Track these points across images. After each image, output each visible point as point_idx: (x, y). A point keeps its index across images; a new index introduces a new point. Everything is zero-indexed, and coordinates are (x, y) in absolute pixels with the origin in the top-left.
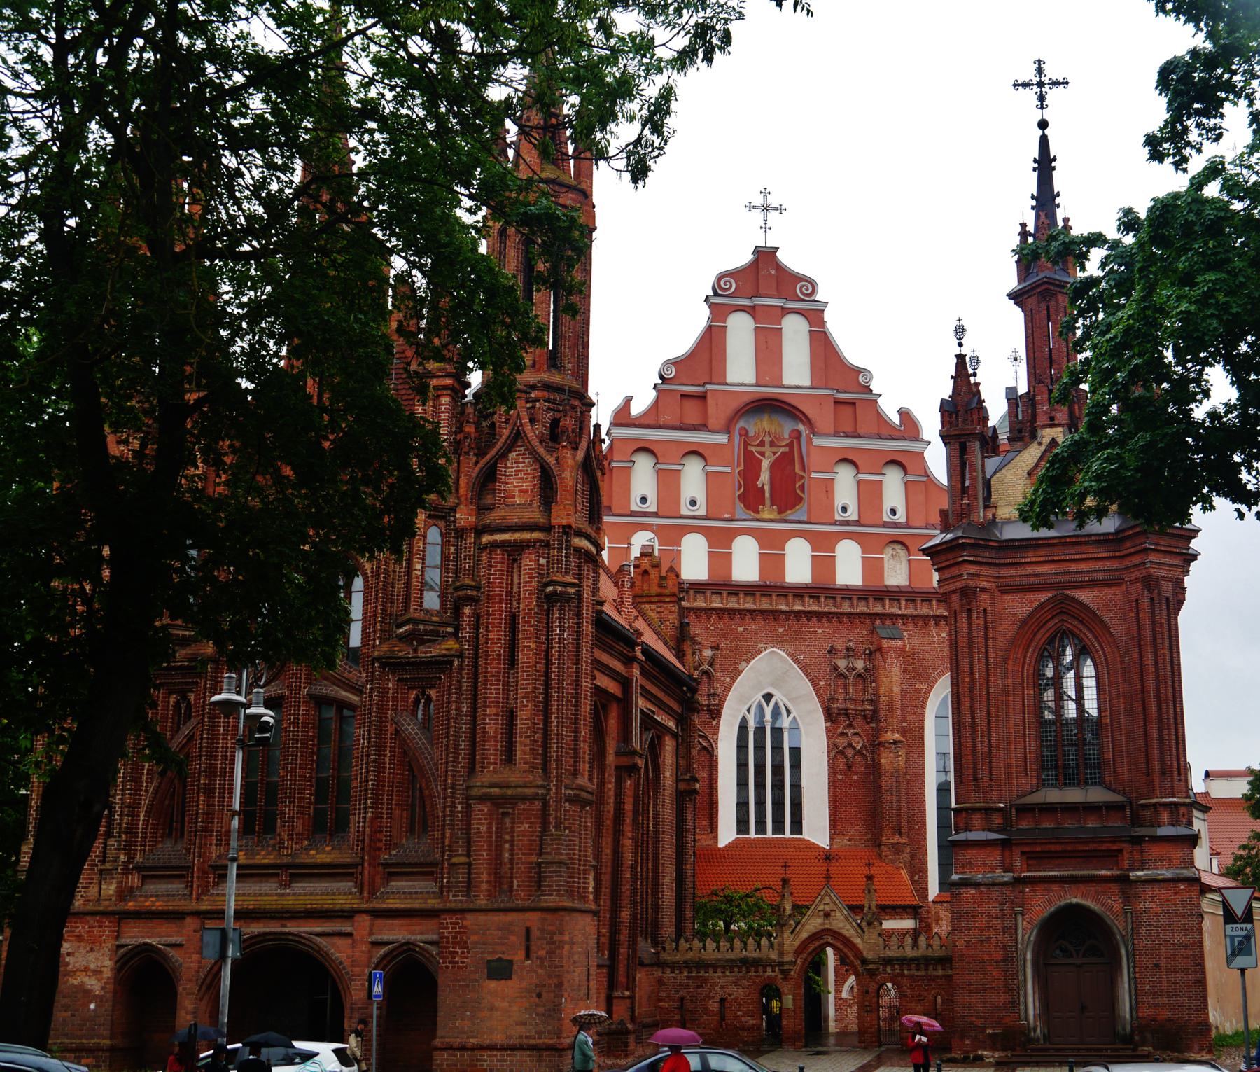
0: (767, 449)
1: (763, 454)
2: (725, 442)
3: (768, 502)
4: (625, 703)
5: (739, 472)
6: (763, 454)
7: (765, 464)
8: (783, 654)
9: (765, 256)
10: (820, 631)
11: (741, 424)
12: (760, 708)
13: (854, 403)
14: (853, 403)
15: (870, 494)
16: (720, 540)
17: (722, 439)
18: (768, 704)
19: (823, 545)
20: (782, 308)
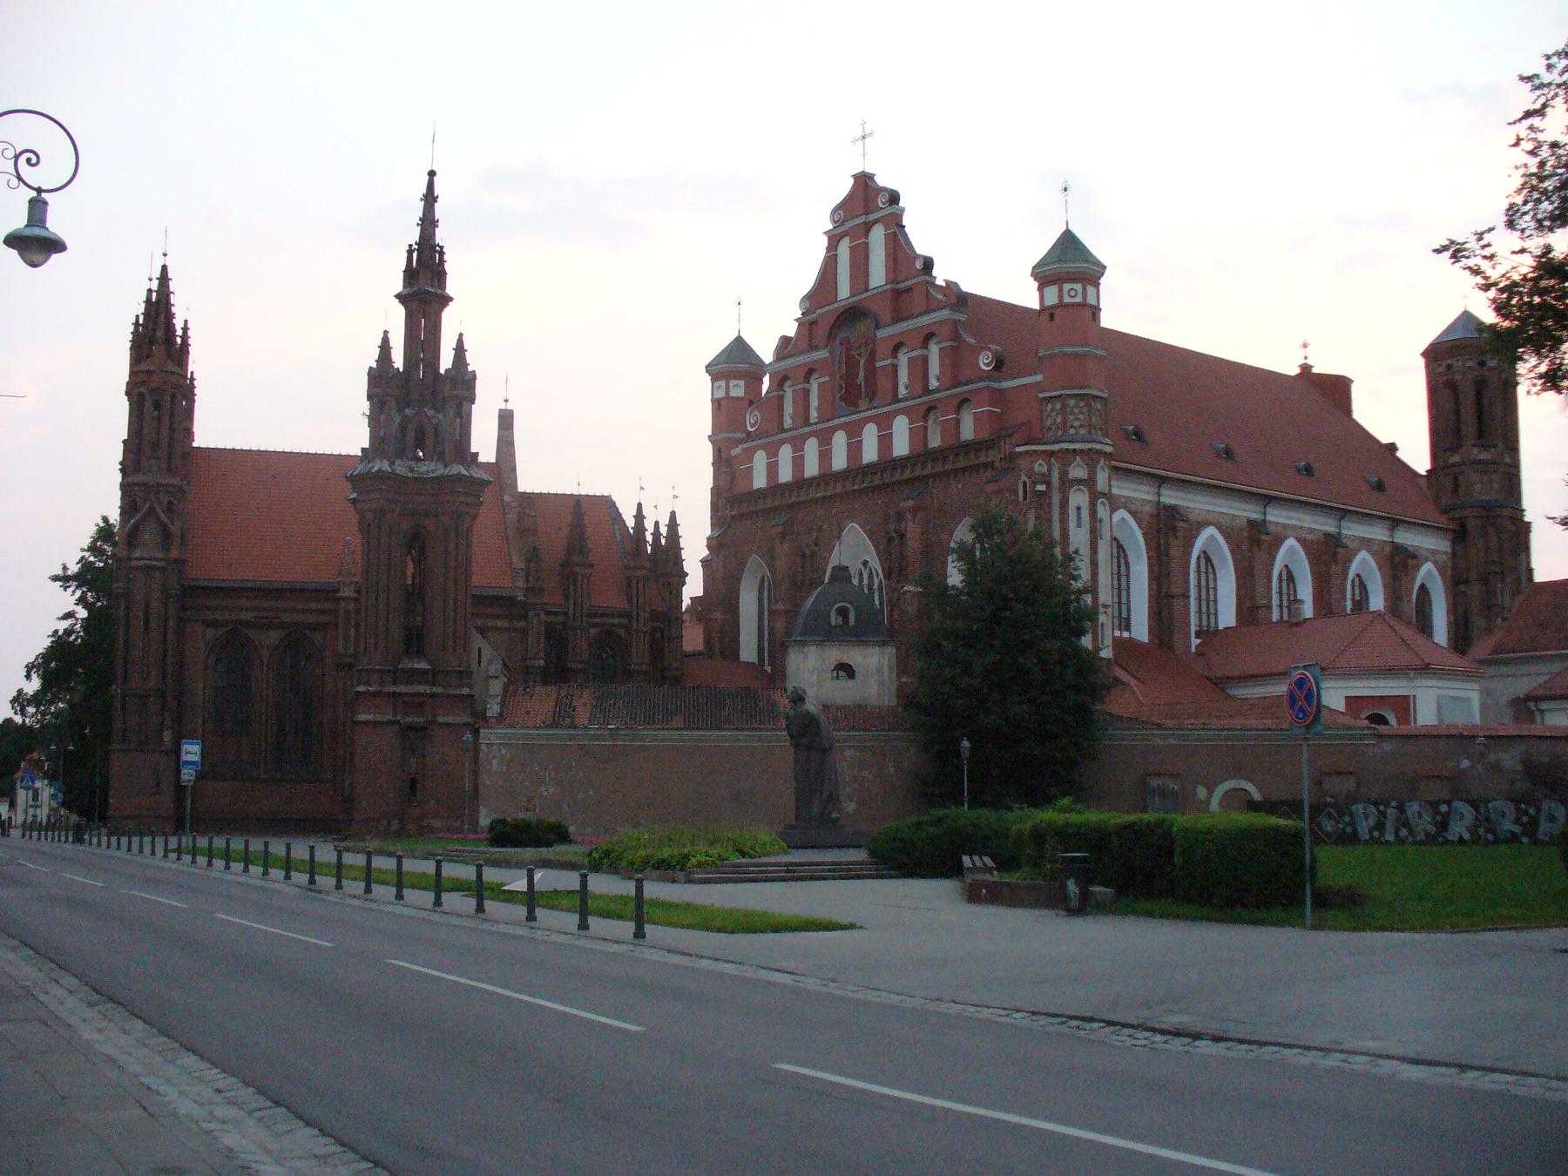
0: (863, 350)
1: (860, 355)
2: (827, 355)
3: (863, 395)
4: (336, 625)
5: (840, 377)
6: (860, 355)
7: (862, 363)
8: (857, 527)
9: (864, 182)
10: (880, 502)
11: (843, 334)
12: (861, 574)
13: (911, 289)
14: (909, 290)
15: (920, 367)
16: (825, 440)
17: (822, 354)
18: (866, 568)
19: (884, 423)
20: (866, 223)
